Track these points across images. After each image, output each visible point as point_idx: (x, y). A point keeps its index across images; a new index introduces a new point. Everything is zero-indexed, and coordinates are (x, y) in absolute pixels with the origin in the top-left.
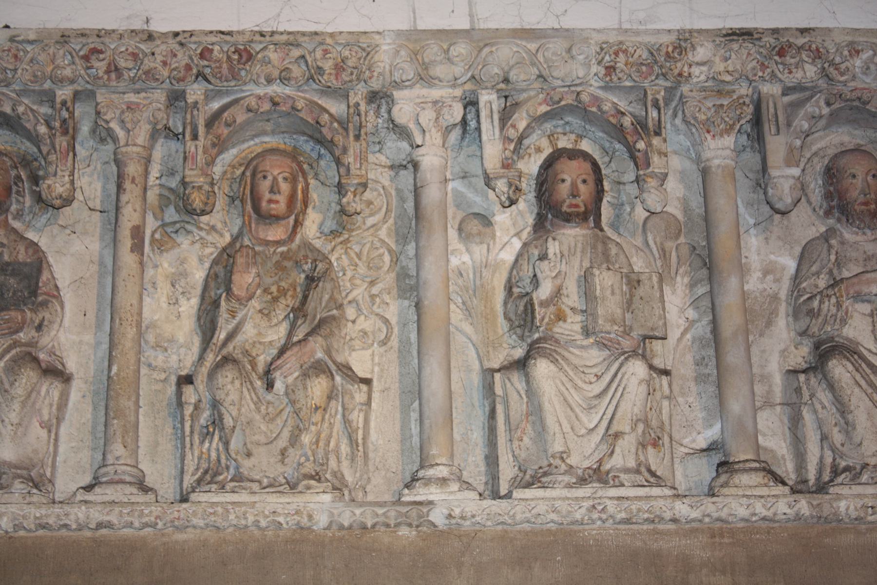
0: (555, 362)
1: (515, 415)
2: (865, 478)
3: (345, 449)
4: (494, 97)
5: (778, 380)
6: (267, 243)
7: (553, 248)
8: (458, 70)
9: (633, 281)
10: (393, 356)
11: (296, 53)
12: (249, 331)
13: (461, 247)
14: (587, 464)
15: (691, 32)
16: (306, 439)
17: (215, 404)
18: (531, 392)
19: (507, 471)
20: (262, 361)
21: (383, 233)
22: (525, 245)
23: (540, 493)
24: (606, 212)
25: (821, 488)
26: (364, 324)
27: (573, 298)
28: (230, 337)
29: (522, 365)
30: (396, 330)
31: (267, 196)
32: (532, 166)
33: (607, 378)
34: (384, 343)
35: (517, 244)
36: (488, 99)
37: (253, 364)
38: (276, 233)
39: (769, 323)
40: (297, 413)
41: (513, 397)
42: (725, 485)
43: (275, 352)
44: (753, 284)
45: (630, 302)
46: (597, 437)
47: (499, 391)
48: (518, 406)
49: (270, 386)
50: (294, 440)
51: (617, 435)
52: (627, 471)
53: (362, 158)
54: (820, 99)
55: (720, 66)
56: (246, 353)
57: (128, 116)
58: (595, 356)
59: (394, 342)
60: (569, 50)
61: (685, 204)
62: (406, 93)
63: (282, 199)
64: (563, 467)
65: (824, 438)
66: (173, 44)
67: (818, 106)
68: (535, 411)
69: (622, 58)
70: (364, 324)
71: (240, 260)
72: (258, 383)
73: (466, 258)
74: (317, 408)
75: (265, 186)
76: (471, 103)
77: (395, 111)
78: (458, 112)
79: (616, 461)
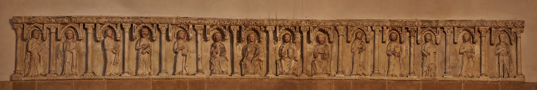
0: (284, 60)
1: (279, 67)
2: (317, 75)
3: (260, 69)
4: (278, 27)
5: (311, 62)
6: (251, 44)
7: (285, 46)
8: (274, 24)
9: (294, 50)
10: (266, 58)
11: (255, 22)
12: (249, 56)
13: (274, 44)
14: (287, 72)
15: (302, 20)
16: (256, 69)
17: (246, 64)
18: (281, 64)
19: (278, 72)
20: (251, 59)
21: (265, 43)
22: (282, 45)
23: (282, 75)
24: (291, 41)
25: (312, 76)
26: (262, 54)
27: (287, 52)
28: (247, 56)
29: (280, 60)
30: (266, 55)
31: (251, 39)
32: (282, 35)
33: (290, 62)
34: (265, 56)
35: (281, 44)
36: (278, 28)
37: (250, 59)
38: (253, 43)
39: (311, 55)
40: (255, 66)
41: (279, 64)
42: (301, 75)
43: (252, 58)
44: (308, 50)
45: (293, 53)
46: (288, 69)
47: (278, 63)
48: (280, 65)
49: (251, 63)
50: (254, 69)
51: (291, 69)
52: (291, 73)
53: (262, 35)
54: (317, 28)
55: (305, 24)
56: (249, 58)
57: (234, 29)
58: (289, 59)
59: (266, 56)
60: (287, 22)
61: (301, 39)
62: (268, 27)
63: (253, 39)
64: (284, 72)
65: (314, 70)
66: (240, 20)
67: (317, 29)
68: (282, 66)
69: (294, 23)
70: (262, 54)
71: (248, 47)
72: (251, 62)
73: (275, 46)
74: (257, 65)
75: (251, 38)
76: (276, 28)
77: (267, 28)
78: (274, 29)
79: (290, 72)
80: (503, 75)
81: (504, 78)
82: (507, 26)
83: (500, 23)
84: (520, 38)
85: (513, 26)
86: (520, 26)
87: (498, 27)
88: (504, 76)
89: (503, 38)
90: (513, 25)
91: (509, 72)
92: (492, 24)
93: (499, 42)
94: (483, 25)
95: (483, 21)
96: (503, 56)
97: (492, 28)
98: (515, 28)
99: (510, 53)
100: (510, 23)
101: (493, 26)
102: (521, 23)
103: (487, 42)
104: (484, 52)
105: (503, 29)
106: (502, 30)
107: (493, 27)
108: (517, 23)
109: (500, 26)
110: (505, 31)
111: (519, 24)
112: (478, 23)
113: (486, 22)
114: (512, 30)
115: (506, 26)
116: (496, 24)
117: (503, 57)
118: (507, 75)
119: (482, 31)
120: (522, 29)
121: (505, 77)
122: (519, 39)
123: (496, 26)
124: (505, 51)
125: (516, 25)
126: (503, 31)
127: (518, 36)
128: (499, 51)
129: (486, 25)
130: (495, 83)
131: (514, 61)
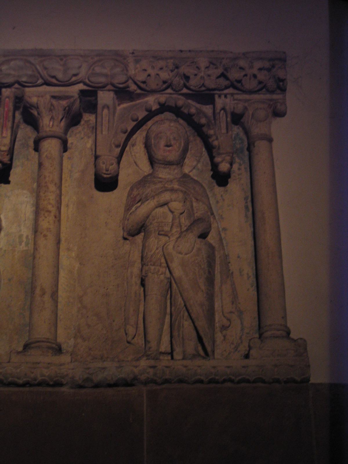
80: (165, 346)
81: (172, 358)
82: (187, 78)
83: (144, 64)
84: (270, 140)
85: (223, 82)
86: (261, 76)
87: (133, 87)
88: (171, 354)
89: (163, 143)
90: (220, 71)
91: (201, 323)
92: (98, 70)
93: (145, 168)
94: (44, 73)
95: (43, 55)
96: (162, 233)
97: (101, 94)
98: (231, 90)
99: (214, 225)
100: (203, 63)
101: (103, 80)
102: (267, 65)
103: (77, 175)
104: (51, 218)
105: (162, 98)
106: (163, 108)
107: (103, 87)
108: (242, 63)
109: (141, 77)
110: (177, 111)
111: (251, 67)
112: (12, 63)
113: (63, 57)
114: (219, 102)
115: (178, 81)
116: (118, 70)
117: (164, 239)
118: (192, 345)
119: (42, 108)
120: (275, 97)
121: (176, 356)
122: (261, 146)
123: (119, 80)
124: (176, 205)
125: (234, 75)
126: (168, 115)
127: (256, 130)
128: (143, 210)
129: (60, 76)
130: (110, 391)
131: (241, 271)
